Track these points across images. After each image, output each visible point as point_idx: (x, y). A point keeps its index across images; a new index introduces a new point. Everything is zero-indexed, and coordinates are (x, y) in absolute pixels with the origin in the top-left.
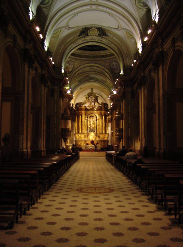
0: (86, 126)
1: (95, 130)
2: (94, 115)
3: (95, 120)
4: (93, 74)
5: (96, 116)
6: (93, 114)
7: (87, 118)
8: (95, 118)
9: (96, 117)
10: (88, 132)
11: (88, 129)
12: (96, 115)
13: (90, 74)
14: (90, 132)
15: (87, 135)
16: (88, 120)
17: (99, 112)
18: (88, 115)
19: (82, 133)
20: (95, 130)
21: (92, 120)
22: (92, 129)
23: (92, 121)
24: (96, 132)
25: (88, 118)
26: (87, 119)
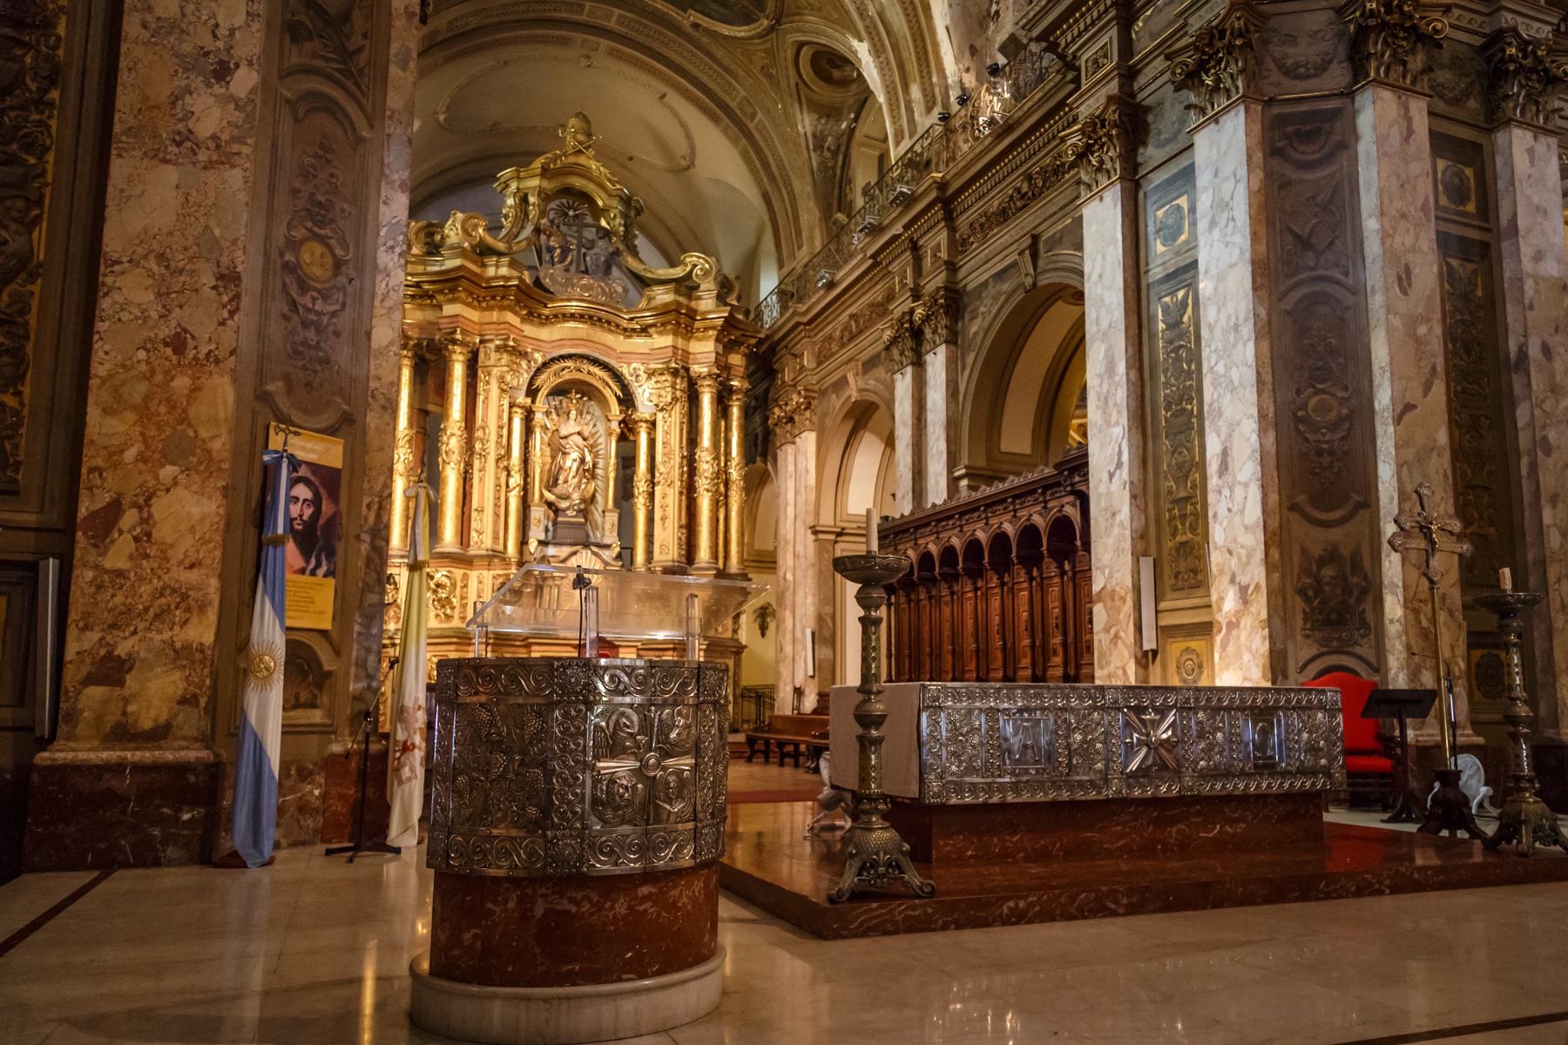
0: (516, 480)
1: (611, 537)
3: (615, 426)
5: (625, 387)
6: (595, 362)
7: (532, 392)
8: (615, 408)
9: (627, 401)
10: (533, 545)
12: (625, 370)
16: (539, 417)
17: (667, 340)
18: (539, 358)
19: (463, 560)
21: (569, 427)
25: (541, 404)
26: (529, 400)
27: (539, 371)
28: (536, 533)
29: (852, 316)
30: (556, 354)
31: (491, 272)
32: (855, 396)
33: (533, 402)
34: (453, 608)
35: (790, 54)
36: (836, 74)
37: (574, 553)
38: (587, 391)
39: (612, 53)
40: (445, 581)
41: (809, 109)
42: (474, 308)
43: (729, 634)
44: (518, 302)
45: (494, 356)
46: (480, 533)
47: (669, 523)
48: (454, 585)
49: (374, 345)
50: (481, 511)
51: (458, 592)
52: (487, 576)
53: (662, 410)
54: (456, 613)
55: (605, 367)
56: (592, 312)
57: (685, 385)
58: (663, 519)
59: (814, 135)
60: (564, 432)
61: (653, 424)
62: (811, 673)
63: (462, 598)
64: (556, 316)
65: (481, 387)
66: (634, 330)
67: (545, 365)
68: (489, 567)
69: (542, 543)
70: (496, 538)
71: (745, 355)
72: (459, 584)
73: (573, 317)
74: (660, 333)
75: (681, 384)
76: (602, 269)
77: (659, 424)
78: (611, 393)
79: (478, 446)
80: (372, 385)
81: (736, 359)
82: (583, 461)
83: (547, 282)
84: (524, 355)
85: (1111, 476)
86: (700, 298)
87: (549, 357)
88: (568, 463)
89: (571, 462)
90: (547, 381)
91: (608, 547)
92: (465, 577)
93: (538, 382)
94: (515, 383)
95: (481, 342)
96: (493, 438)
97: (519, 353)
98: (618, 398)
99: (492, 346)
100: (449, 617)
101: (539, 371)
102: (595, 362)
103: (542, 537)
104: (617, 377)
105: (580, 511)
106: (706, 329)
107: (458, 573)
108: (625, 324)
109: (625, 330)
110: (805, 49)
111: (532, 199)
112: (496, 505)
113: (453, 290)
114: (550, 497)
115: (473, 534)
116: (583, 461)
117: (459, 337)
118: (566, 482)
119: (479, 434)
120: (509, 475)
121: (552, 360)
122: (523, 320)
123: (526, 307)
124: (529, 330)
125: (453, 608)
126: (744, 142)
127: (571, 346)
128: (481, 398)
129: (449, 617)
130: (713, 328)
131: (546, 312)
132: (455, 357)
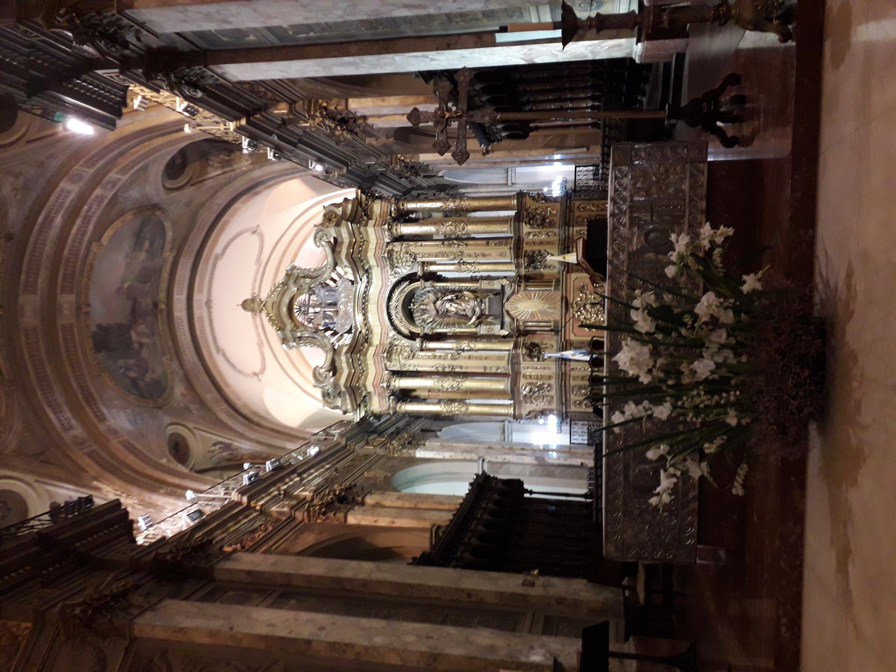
0: (465, 345)
2: (398, 297)
3: (428, 284)
4: (66, 300)
6: (390, 298)
7: (412, 336)
11: (483, 330)
13: (66, 317)
14: (507, 319)
15: (521, 339)
18: (392, 333)
20: (497, 286)
22: (485, 306)
23: (439, 302)
24: (505, 282)
26: (418, 340)
27: (400, 332)
28: (497, 330)
29: (337, 144)
30: (388, 323)
31: (344, 365)
32: (392, 140)
33: (418, 335)
34: (544, 384)
35: (175, 194)
36: (179, 161)
37: (508, 312)
38: (409, 299)
39: (201, 291)
40: (527, 389)
41: (206, 174)
42: (367, 374)
43: (558, 205)
44: (360, 351)
45: (393, 363)
46: (498, 368)
47: (486, 252)
48: (530, 384)
49: (400, 663)
50: (485, 368)
51: (534, 381)
52: (523, 364)
53: (415, 259)
54: (548, 382)
55: (392, 291)
56: (360, 303)
57: (396, 244)
58: (484, 255)
59: (222, 168)
60: (434, 312)
61: (423, 263)
62: (585, 149)
63: (537, 378)
64: (366, 325)
65: (411, 369)
66: (368, 277)
67: (395, 328)
68: (518, 364)
69: (502, 328)
70: (500, 358)
71: (373, 201)
72: (530, 381)
73: (365, 318)
74: (368, 262)
75: (397, 247)
76: (333, 293)
77: (424, 259)
78: (407, 287)
79: (447, 370)
80: (422, 665)
81: (377, 207)
82: (451, 300)
83: (347, 328)
84: (391, 345)
85: (432, 60)
86: (341, 236)
87: (391, 327)
88: (453, 309)
89: (452, 307)
90: (405, 327)
91: (503, 287)
92: (525, 376)
93: (406, 332)
94: (408, 349)
95: (387, 370)
96: (442, 362)
97: (390, 351)
98: (410, 283)
99: (388, 364)
100: (549, 385)
101: (400, 332)
102: (390, 298)
103: (499, 326)
104: (397, 284)
105: (481, 301)
106: (360, 233)
107: (522, 382)
108: (364, 285)
109: (368, 282)
110: (168, 186)
111: (299, 334)
112: (481, 358)
113: (359, 388)
114: (474, 318)
115: (499, 371)
116: (451, 300)
117: (385, 385)
118: (464, 310)
119: (440, 370)
120: (463, 350)
121: (392, 323)
122: (370, 345)
123: (362, 345)
124: (376, 340)
125: (544, 384)
126: (237, 205)
127: (382, 314)
128: (420, 369)
129: (549, 385)
130: (359, 229)
131: (364, 331)
132: (397, 385)
